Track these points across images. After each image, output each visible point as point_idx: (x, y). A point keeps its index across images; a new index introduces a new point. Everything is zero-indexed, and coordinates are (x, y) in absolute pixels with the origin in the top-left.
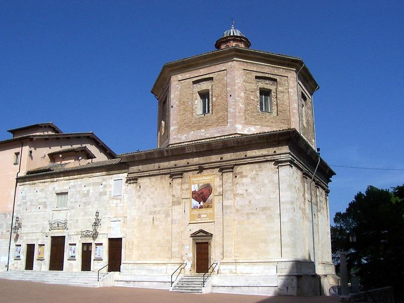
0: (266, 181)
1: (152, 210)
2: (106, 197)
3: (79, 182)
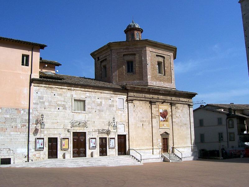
0: (186, 113)
1: (142, 120)
2: (114, 108)
3: (93, 94)
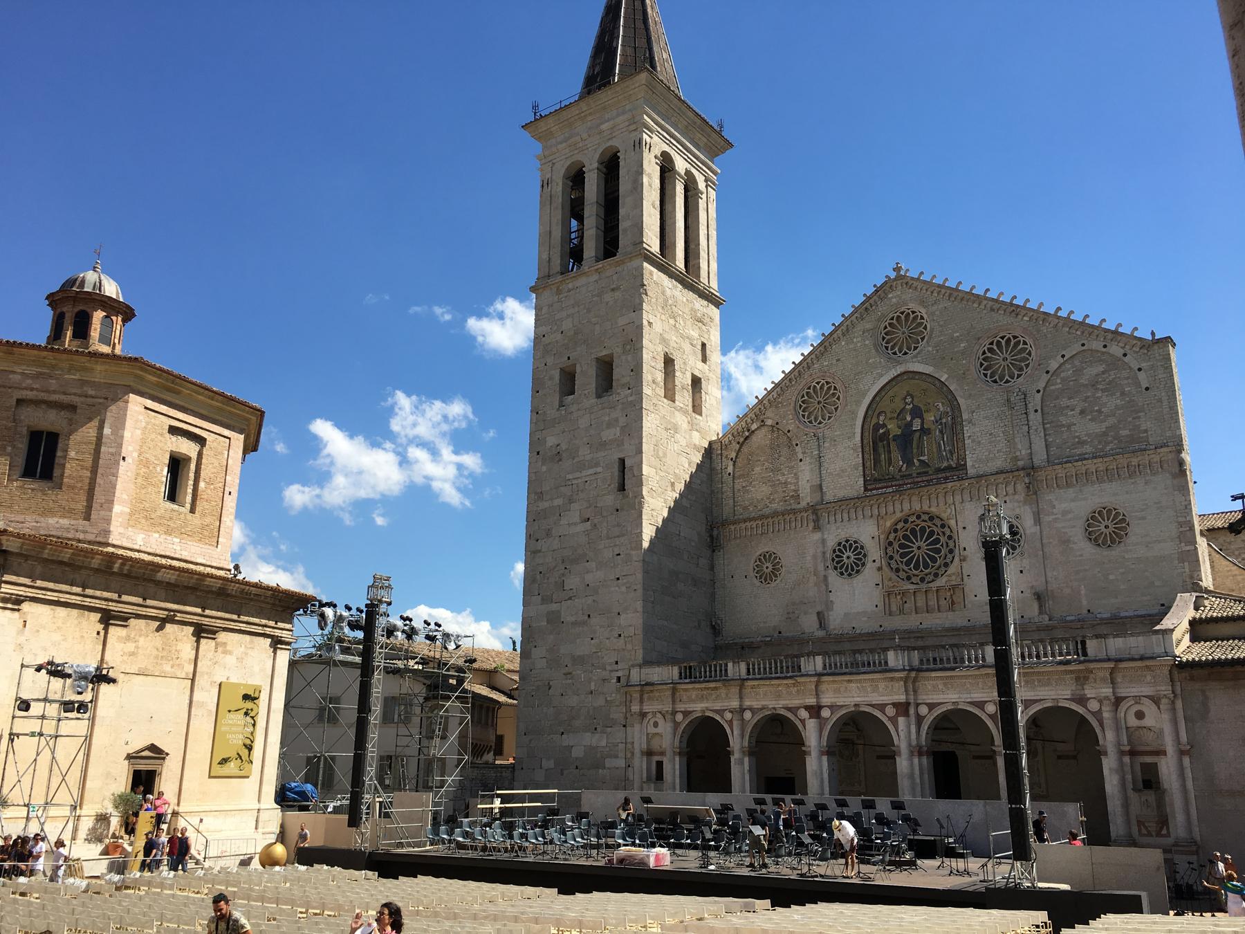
0: (256, 669)
